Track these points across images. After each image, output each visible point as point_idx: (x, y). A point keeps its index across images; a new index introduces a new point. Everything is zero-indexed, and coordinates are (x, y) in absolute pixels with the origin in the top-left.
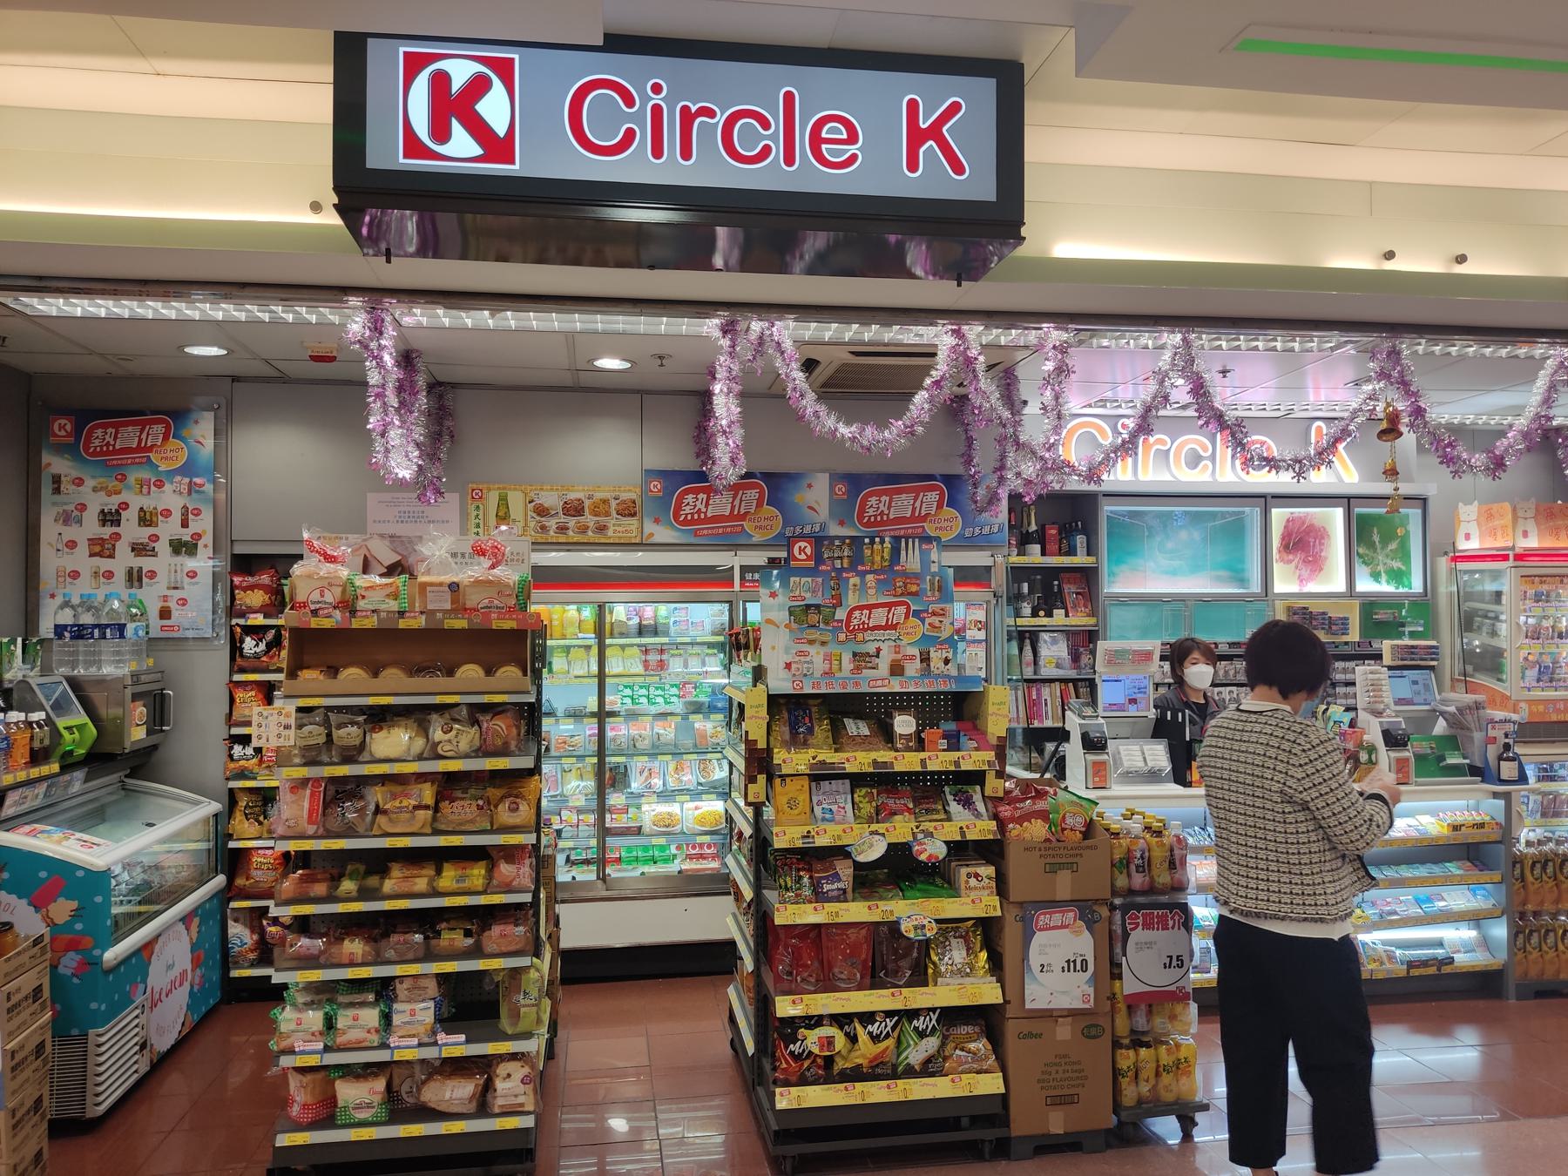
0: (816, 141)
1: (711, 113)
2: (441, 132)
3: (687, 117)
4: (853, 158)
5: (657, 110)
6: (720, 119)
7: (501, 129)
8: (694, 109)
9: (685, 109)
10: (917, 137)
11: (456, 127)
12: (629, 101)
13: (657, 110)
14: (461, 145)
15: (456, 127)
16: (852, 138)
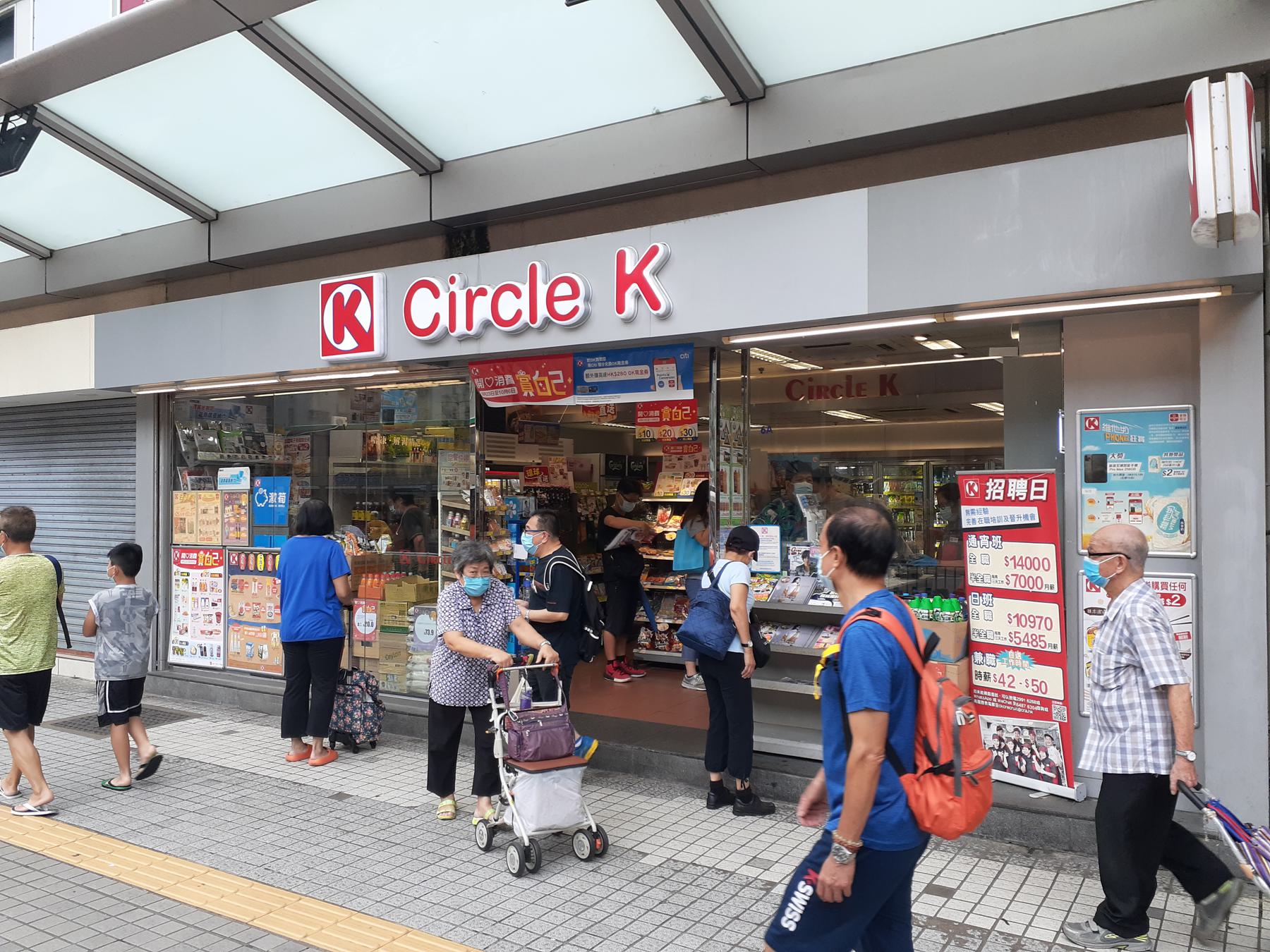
0: (551, 299)
1: (482, 292)
2: (339, 337)
3: (470, 299)
4: (576, 309)
5: (452, 297)
6: (491, 292)
7: (367, 329)
8: (474, 290)
9: (469, 292)
10: (623, 282)
11: (347, 333)
12: (436, 293)
13: (452, 297)
14: (349, 342)
15: (347, 333)
16: (575, 294)
